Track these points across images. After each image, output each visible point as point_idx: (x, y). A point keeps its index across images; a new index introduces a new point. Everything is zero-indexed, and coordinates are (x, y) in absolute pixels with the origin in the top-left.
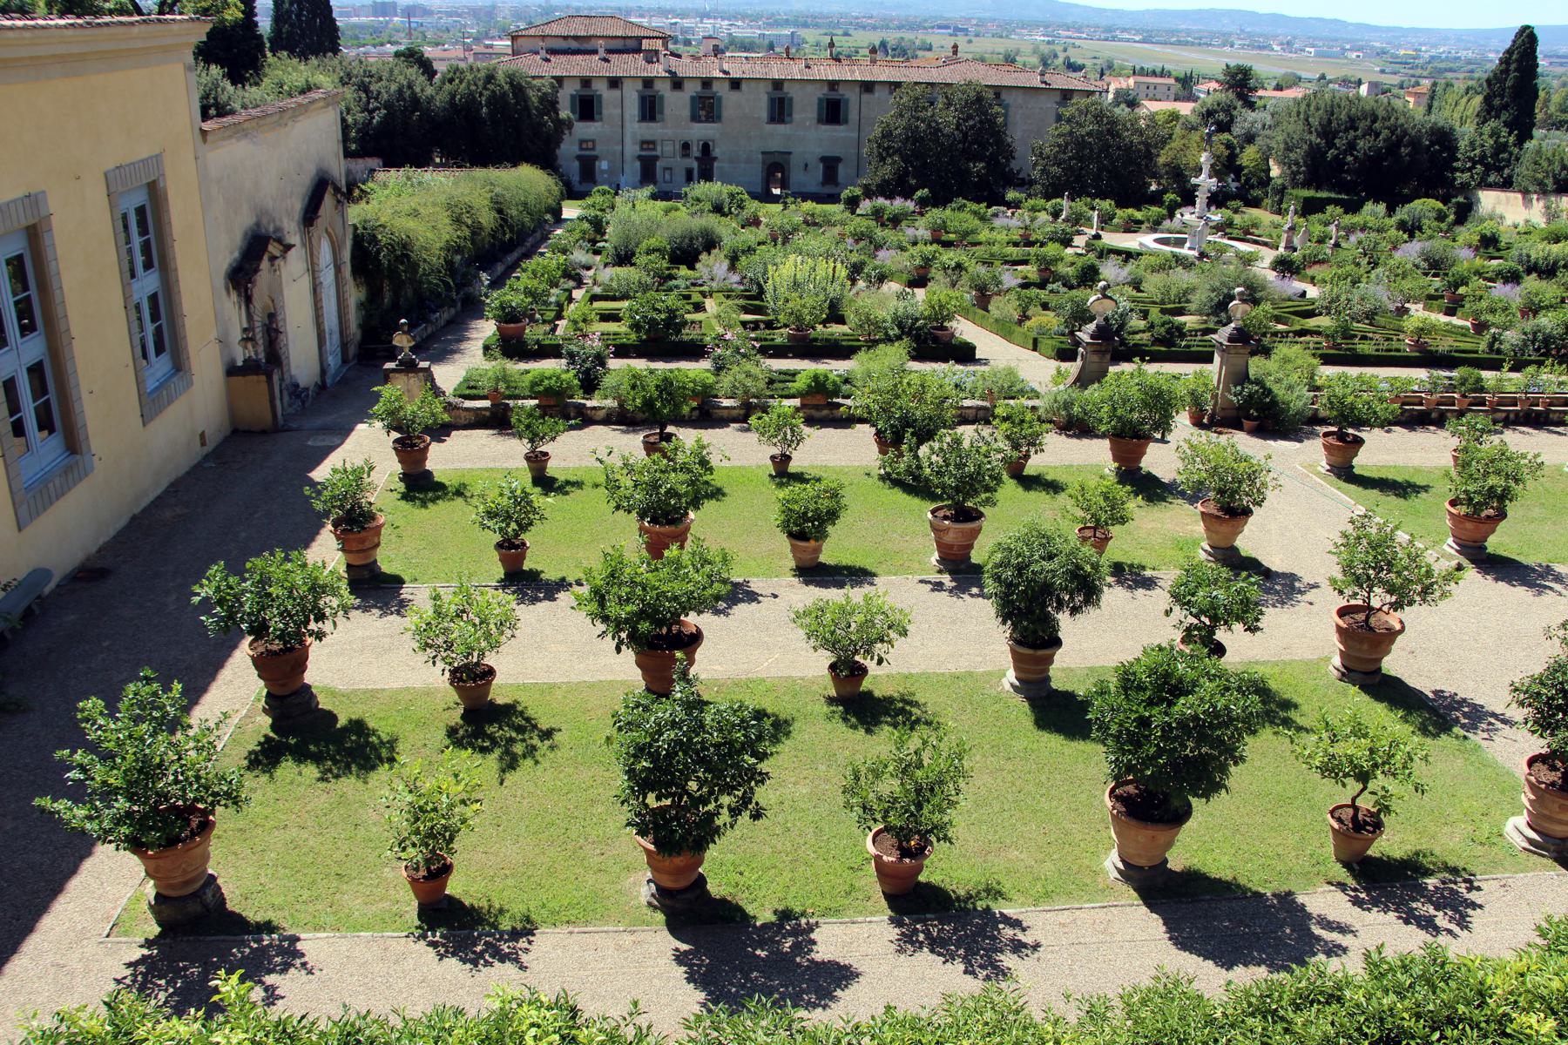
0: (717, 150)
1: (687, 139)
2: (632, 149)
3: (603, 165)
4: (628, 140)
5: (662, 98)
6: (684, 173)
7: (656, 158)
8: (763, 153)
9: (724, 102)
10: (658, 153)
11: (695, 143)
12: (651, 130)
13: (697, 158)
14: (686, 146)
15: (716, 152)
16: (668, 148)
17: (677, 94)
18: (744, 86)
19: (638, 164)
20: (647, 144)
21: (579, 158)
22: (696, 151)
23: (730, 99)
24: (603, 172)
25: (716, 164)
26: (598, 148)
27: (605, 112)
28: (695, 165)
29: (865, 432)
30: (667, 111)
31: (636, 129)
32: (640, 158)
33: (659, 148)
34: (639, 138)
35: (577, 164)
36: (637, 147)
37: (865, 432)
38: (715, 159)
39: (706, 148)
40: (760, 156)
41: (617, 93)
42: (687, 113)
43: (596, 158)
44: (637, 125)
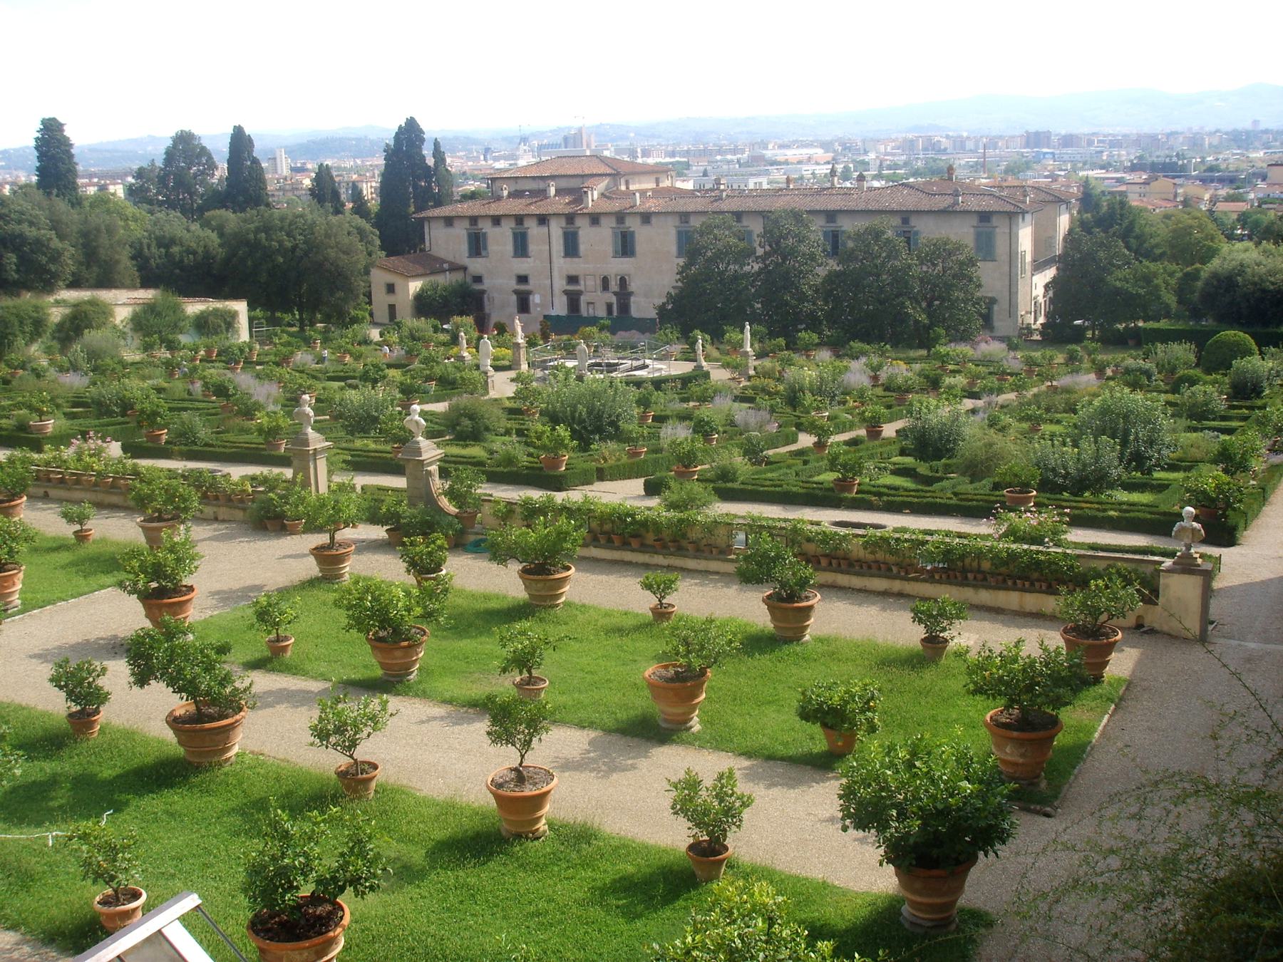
0: (632, 284)
2: (560, 284)
3: (536, 299)
4: (556, 274)
6: (605, 307)
7: (579, 293)
9: (637, 236)
10: (581, 287)
11: (613, 276)
12: (573, 266)
14: (605, 283)
15: (633, 287)
16: (590, 283)
18: (654, 220)
19: (565, 298)
20: (573, 279)
21: (516, 292)
22: (614, 286)
23: (643, 235)
24: (537, 305)
25: (632, 299)
26: (531, 281)
28: (614, 299)
29: (515, 567)
31: (563, 266)
32: (566, 292)
33: (582, 282)
34: (565, 273)
35: (514, 297)
36: (564, 282)
37: (515, 567)
38: (631, 294)
43: (529, 293)
44: (562, 260)
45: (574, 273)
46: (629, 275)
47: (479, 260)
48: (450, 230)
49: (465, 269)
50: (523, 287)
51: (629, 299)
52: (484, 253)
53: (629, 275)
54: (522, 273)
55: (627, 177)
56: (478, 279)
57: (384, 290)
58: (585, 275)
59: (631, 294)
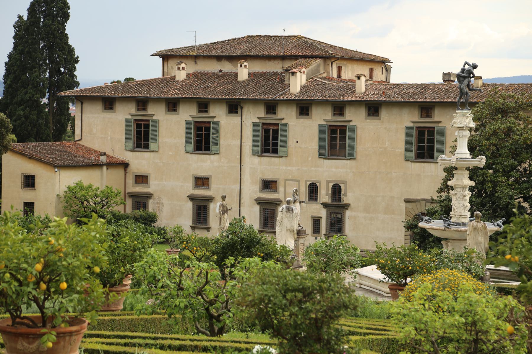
0: (349, 194)
1: (314, 180)
4: (246, 177)
5: (285, 126)
8: (407, 201)
10: (279, 195)
13: (325, 205)
15: (348, 198)
17: (304, 122)
22: (324, 196)
25: (348, 213)
27: (222, 142)
28: (323, 213)
30: (291, 143)
33: (281, 189)
36: (257, 187)
38: (346, 207)
39: (337, 190)
40: (403, 204)
41: (235, 119)
42: (314, 145)
45: (270, 177)
46: (345, 182)
47: (146, 155)
48: (108, 115)
49: (125, 165)
50: (202, 192)
51: (343, 214)
52: (152, 146)
53: (345, 182)
54: (202, 173)
55: (340, 63)
56: (142, 179)
57: (19, 182)
58: (286, 180)
59: (346, 207)
